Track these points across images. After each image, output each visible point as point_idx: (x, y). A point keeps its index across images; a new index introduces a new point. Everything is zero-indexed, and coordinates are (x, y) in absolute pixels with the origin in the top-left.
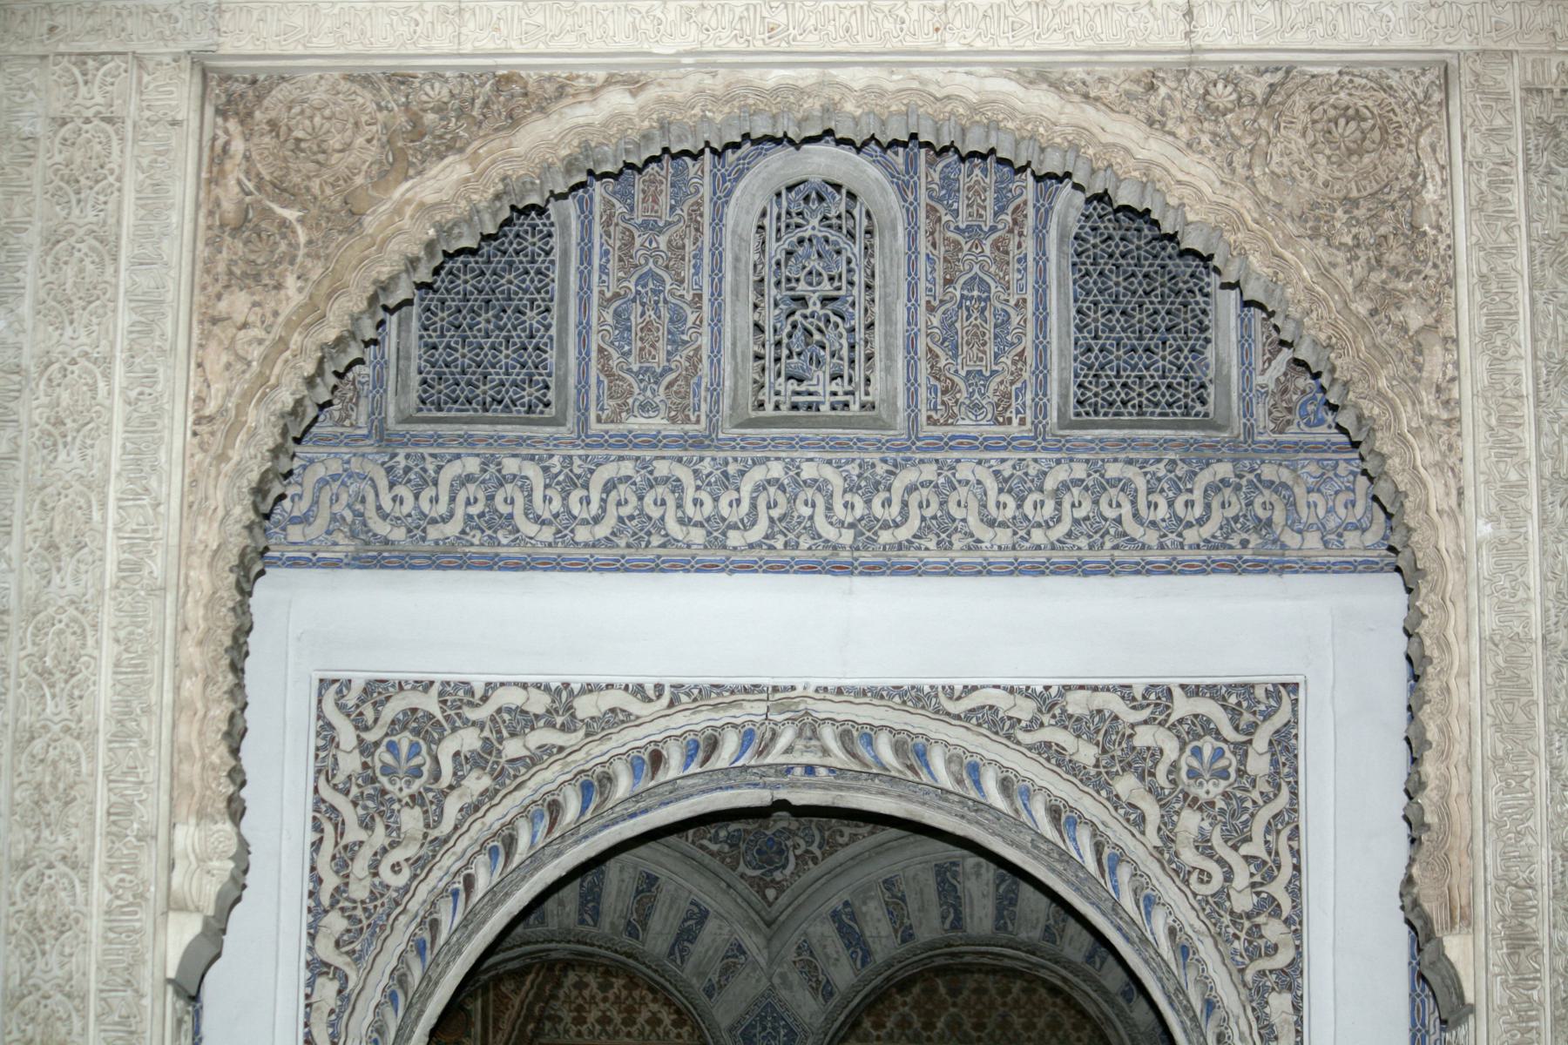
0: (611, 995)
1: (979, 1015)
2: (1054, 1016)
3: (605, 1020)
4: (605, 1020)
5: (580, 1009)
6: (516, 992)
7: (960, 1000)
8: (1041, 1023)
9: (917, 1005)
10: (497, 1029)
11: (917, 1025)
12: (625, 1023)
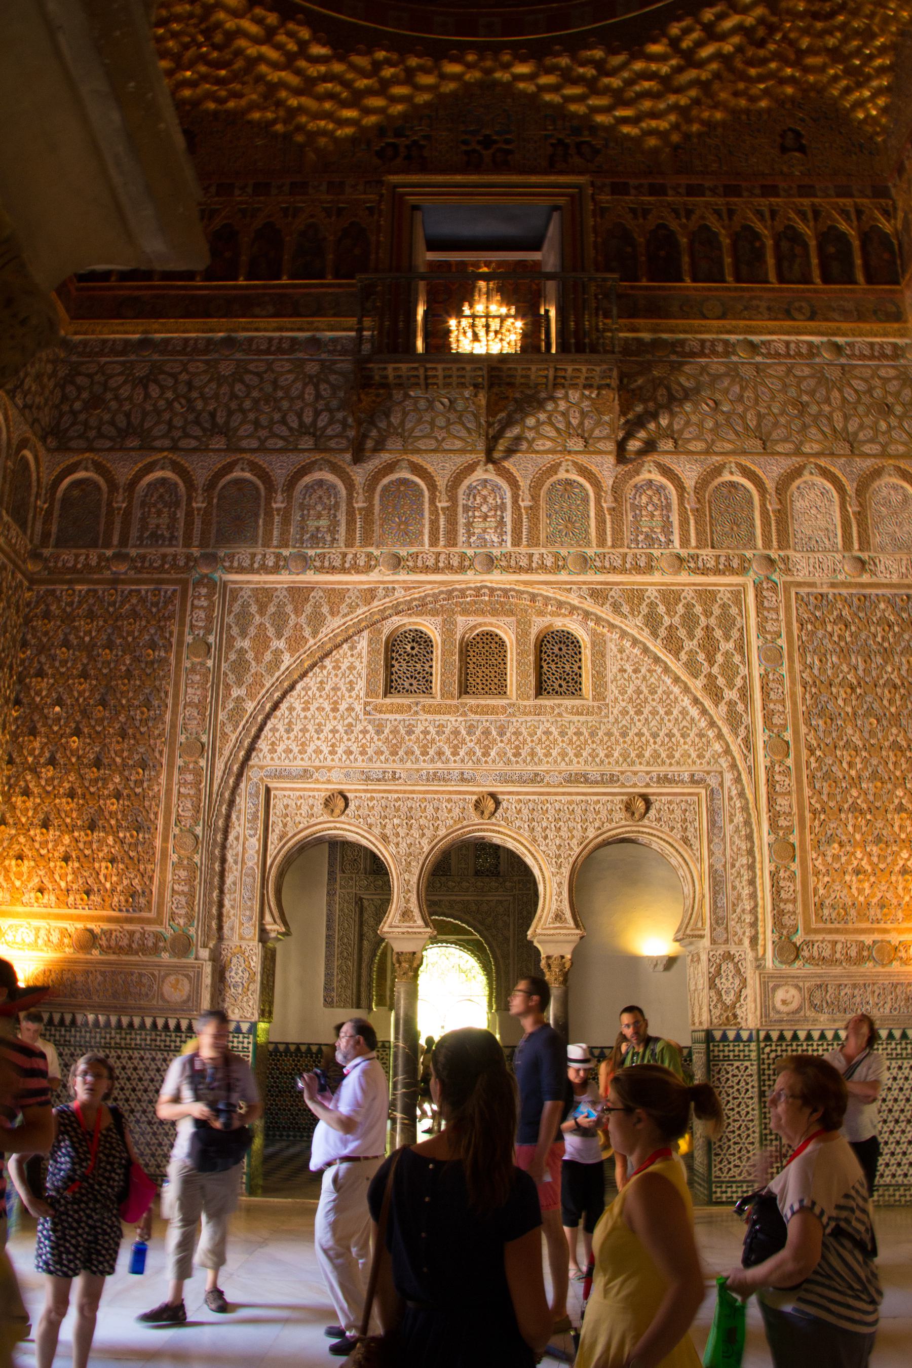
0: (292, 735)
1: (517, 747)
2: (563, 749)
3: (288, 751)
4: (288, 751)
5: (273, 744)
6: (234, 731)
7: (505, 738)
8: (554, 753)
9: (479, 741)
10: (221, 754)
11: (479, 753)
12: (300, 752)
